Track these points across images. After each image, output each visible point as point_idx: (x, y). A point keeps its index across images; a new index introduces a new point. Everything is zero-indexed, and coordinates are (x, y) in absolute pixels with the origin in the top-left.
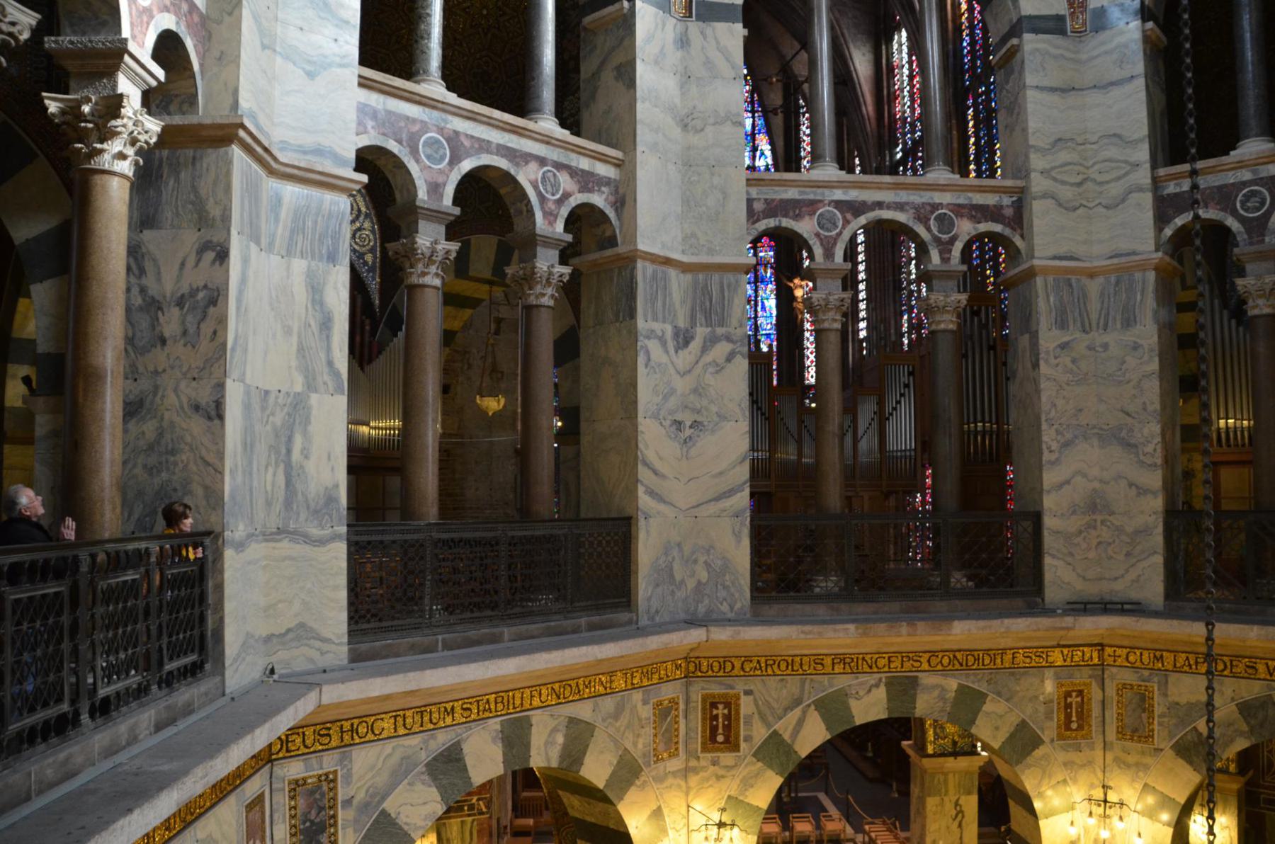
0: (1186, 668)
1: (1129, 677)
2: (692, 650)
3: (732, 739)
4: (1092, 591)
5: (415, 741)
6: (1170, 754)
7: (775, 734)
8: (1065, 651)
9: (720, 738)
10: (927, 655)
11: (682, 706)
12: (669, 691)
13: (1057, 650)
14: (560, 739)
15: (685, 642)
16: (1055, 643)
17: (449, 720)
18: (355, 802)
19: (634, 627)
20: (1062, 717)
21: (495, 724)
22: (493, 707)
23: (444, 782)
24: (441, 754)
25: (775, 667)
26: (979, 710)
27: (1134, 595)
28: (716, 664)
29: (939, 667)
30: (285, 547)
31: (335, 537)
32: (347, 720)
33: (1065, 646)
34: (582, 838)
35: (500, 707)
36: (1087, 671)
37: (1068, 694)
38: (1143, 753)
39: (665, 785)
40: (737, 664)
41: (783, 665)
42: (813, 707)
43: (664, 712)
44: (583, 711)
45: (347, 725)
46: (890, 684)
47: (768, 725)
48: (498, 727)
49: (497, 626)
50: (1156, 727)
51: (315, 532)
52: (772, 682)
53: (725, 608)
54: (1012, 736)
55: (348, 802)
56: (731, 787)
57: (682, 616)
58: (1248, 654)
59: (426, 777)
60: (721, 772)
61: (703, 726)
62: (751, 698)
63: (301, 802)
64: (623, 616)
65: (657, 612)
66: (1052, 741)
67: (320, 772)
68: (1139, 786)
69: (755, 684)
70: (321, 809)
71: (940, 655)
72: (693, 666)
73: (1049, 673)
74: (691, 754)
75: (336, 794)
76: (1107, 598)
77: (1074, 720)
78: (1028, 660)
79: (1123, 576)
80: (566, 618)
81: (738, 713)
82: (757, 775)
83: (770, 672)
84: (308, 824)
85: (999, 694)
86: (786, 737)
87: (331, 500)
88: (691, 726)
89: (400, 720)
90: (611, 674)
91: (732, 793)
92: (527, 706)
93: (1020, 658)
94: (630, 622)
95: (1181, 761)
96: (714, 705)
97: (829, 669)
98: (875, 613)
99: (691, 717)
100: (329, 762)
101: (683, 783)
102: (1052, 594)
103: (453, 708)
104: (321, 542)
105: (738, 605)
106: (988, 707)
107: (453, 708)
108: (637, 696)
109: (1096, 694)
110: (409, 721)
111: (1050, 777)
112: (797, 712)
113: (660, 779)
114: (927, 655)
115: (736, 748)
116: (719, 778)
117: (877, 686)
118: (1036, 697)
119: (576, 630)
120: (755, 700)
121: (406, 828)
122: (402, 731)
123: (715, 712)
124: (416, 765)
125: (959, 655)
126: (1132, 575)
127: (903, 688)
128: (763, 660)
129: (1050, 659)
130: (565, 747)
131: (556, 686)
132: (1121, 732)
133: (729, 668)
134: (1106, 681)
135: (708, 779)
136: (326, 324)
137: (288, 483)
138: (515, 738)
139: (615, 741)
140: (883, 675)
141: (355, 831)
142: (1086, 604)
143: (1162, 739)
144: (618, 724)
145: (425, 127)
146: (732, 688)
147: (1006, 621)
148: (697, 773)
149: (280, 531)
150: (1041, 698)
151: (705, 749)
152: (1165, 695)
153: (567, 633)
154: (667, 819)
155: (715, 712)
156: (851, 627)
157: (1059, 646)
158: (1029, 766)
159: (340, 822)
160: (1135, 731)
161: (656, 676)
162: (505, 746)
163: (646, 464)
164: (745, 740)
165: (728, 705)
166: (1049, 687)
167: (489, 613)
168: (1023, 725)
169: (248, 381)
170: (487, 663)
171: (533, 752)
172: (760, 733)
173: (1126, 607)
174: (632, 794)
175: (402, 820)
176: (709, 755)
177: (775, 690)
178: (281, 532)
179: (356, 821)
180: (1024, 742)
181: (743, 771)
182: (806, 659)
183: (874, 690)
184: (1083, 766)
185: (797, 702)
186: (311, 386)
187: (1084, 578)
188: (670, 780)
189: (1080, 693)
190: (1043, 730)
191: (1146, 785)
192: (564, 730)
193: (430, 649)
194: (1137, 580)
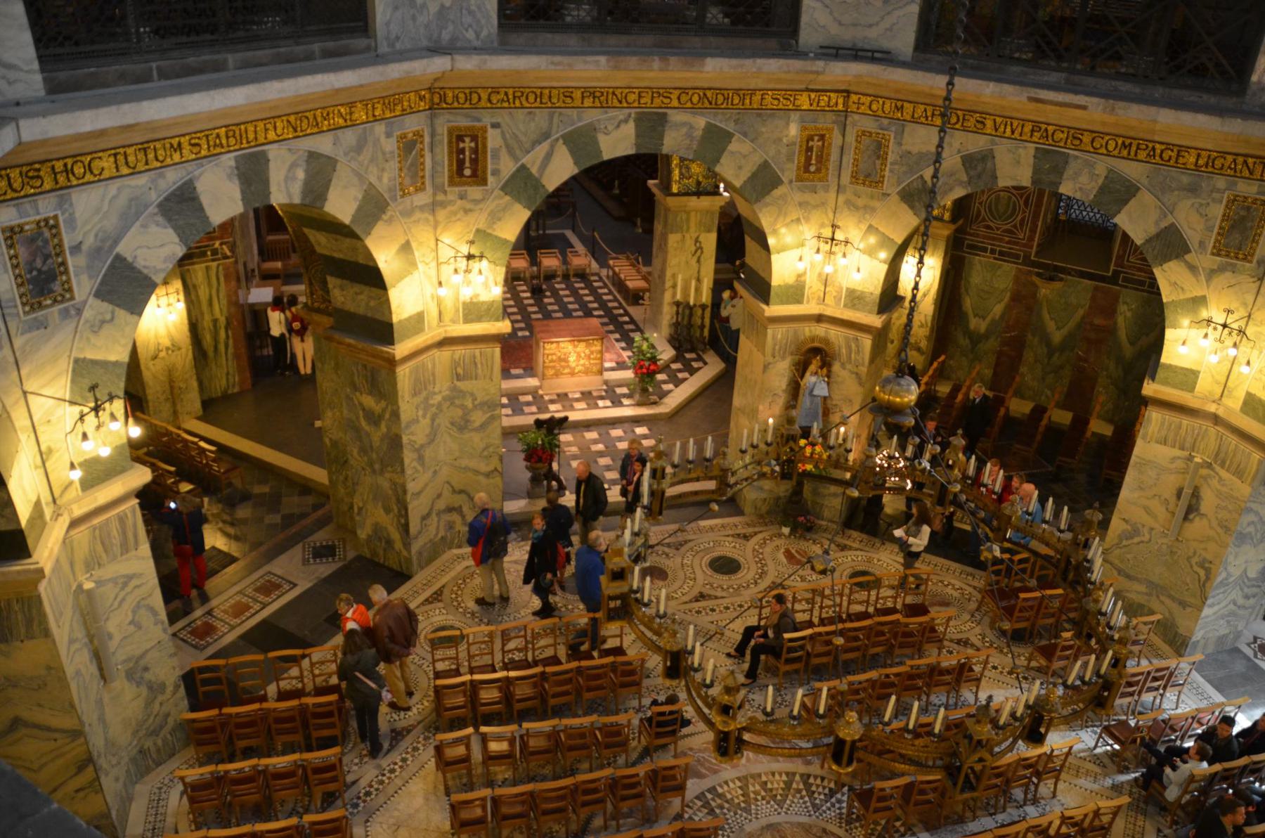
0: (923, 120)
1: (869, 125)
2: (436, 80)
3: (479, 173)
4: (846, 36)
5: (142, 180)
6: (895, 198)
7: (523, 168)
8: (813, 95)
9: (467, 172)
10: (677, 92)
11: (427, 139)
12: (413, 124)
13: (805, 94)
14: (301, 174)
15: (429, 71)
16: (803, 87)
17: (177, 157)
18: (85, 247)
19: (373, 54)
20: (803, 159)
21: (229, 160)
22: (224, 141)
23: (181, 222)
24: (173, 194)
25: (523, 99)
26: (724, 150)
27: (886, 44)
28: (462, 96)
29: (689, 105)
32: (58, 159)
33: (812, 91)
34: (332, 275)
35: (232, 141)
36: (831, 117)
37: (810, 138)
38: (872, 197)
39: (413, 219)
40: (484, 96)
41: (532, 98)
42: (561, 141)
43: (409, 146)
44: (323, 144)
45: (59, 166)
46: (639, 120)
47: (516, 159)
48: (233, 163)
49: (219, 52)
50: (887, 173)
52: (520, 114)
53: (470, 35)
54: (754, 176)
55: (76, 249)
56: (479, 220)
57: (425, 43)
58: (980, 109)
59: (160, 219)
60: (469, 206)
61: (450, 160)
62: (498, 131)
63: (23, 252)
64: (361, 42)
65: (398, 38)
66: (791, 182)
67: (38, 218)
68: (864, 227)
69: (503, 117)
70: (47, 257)
71: (691, 92)
72: (437, 97)
73: (795, 116)
74: (438, 188)
75: (61, 240)
76: (860, 45)
77: (813, 162)
78: (776, 102)
79: (877, 24)
80: (298, 44)
81: (485, 146)
82: (505, 209)
83: (518, 104)
84: (35, 273)
85: (745, 135)
86: (534, 171)
88: (437, 159)
89: (121, 158)
90: (351, 105)
91: (481, 226)
92: (262, 140)
93: (768, 99)
94: (368, 49)
95: (905, 206)
96: (460, 138)
97: (578, 103)
98: (628, 46)
99: (437, 150)
100: (46, 207)
101: (431, 218)
102: (808, 36)
103: (179, 144)
105: (484, 33)
106: (734, 146)
107: (179, 144)
108: (380, 129)
109: (836, 139)
110: (131, 159)
111: (786, 214)
112: (545, 146)
113: (407, 213)
114: (677, 92)
115: (484, 182)
116: (467, 211)
117: (626, 121)
118: (780, 140)
119: (309, 57)
120: (503, 133)
121: (145, 271)
122: (125, 171)
123: (461, 145)
124: (147, 206)
125: (709, 93)
126: (886, 24)
127: (652, 124)
128: (510, 92)
129: (798, 103)
130: (307, 183)
131: (292, 118)
132: (855, 177)
133: (475, 98)
134: (848, 128)
135: (455, 213)
138: (252, 173)
140: (633, 111)
141: (90, 277)
142: (838, 49)
143: (891, 186)
144: (361, 158)
146: (479, 120)
147: (759, 61)
148: (445, 207)
150: (785, 140)
151: (452, 183)
152: (900, 144)
153: (300, 60)
154: (416, 254)
155: (461, 145)
156: (603, 59)
157: (807, 90)
158: (767, 205)
159: (71, 269)
160: (868, 176)
161: (399, 108)
162: (242, 184)
164: (493, 174)
165: (474, 138)
166: (793, 130)
167: (208, 37)
168: (765, 166)
170: (212, 92)
171: (273, 188)
172: (508, 167)
173: (876, 55)
174: (380, 229)
175: (140, 263)
176: (456, 189)
177: (522, 123)
179: (89, 267)
180: (764, 182)
181: (491, 205)
182: (555, 92)
183: (623, 126)
184: (816, 207)
185: (546, 136)
187: (840, 24)
188: (418, 215)
189: (822, 137)
190: (783, 171)
191: (870, 227)
192: (304, 164)
193: (145, 78)
194: (890, 29)
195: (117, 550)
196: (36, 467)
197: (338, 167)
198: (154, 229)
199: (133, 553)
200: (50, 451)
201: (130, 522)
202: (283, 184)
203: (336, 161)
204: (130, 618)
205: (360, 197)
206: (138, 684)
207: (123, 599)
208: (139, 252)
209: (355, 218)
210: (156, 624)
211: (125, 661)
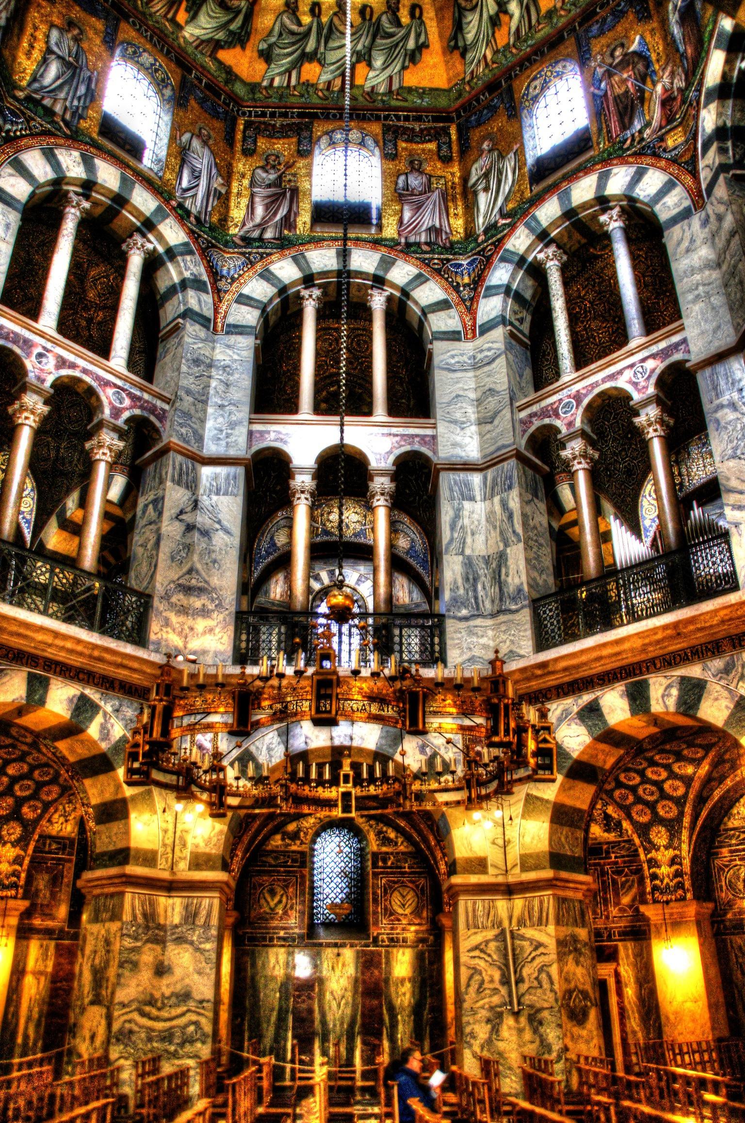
14: (675, 692)
30: (502, 618)
31: (522, 608)
48: (623, 688)
51: (513, 607)
59: (577, 721)
87: (520, 590)
104: (517, 611)
136: (510, 517)
137: (501, 589)
139: (730, 691)
145: (561, 400)
149: (498, 612)
163: (730, 491)
169: (468, 552)
171: (653, 702)
178: (500, 612)
186: (506, 545)
195: (535, 919)
196: (494, 843)
197: (708, 686)
198: (573, 726)
199: (543, 927)
200: (509, 842)
201: (545, 905)
202: (660, 701)
203: (706, 681)
204: (536, 975)
205: (732, 706)
206: (535, 1031)
207: (533, 958)
208: (565, 739)
209: (727, 723)
210: (552, 990)
211: (529, 1006)
